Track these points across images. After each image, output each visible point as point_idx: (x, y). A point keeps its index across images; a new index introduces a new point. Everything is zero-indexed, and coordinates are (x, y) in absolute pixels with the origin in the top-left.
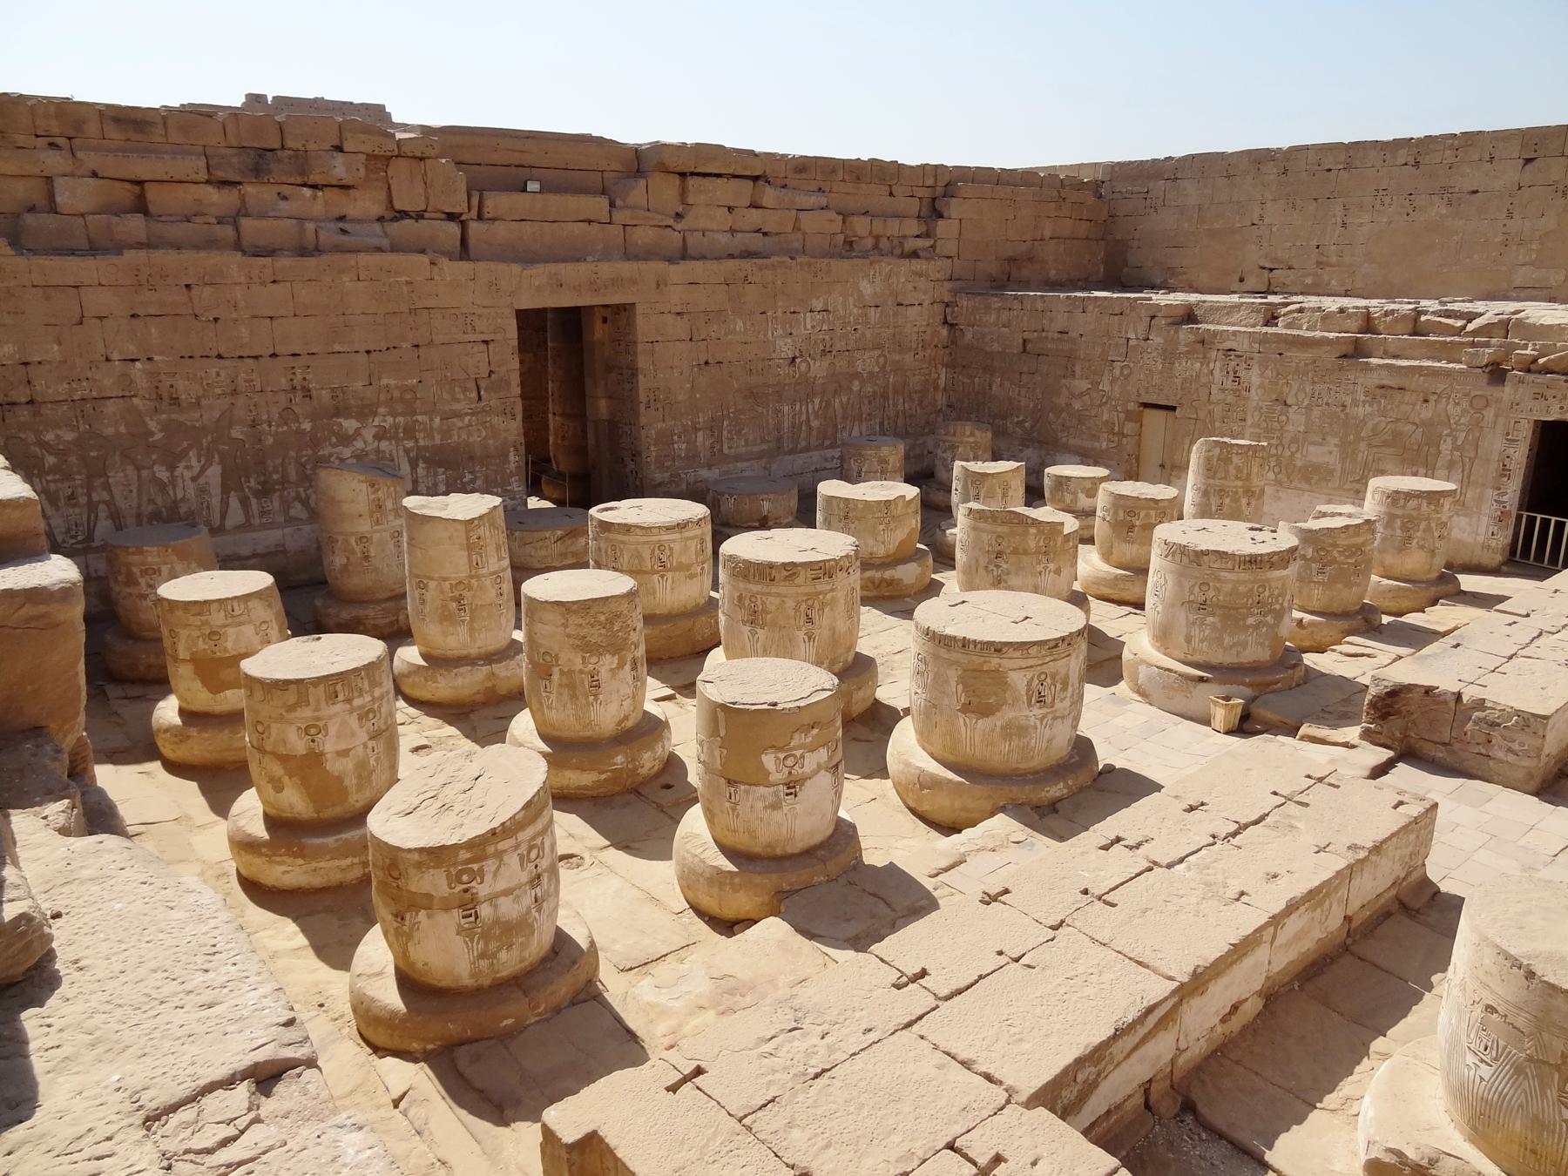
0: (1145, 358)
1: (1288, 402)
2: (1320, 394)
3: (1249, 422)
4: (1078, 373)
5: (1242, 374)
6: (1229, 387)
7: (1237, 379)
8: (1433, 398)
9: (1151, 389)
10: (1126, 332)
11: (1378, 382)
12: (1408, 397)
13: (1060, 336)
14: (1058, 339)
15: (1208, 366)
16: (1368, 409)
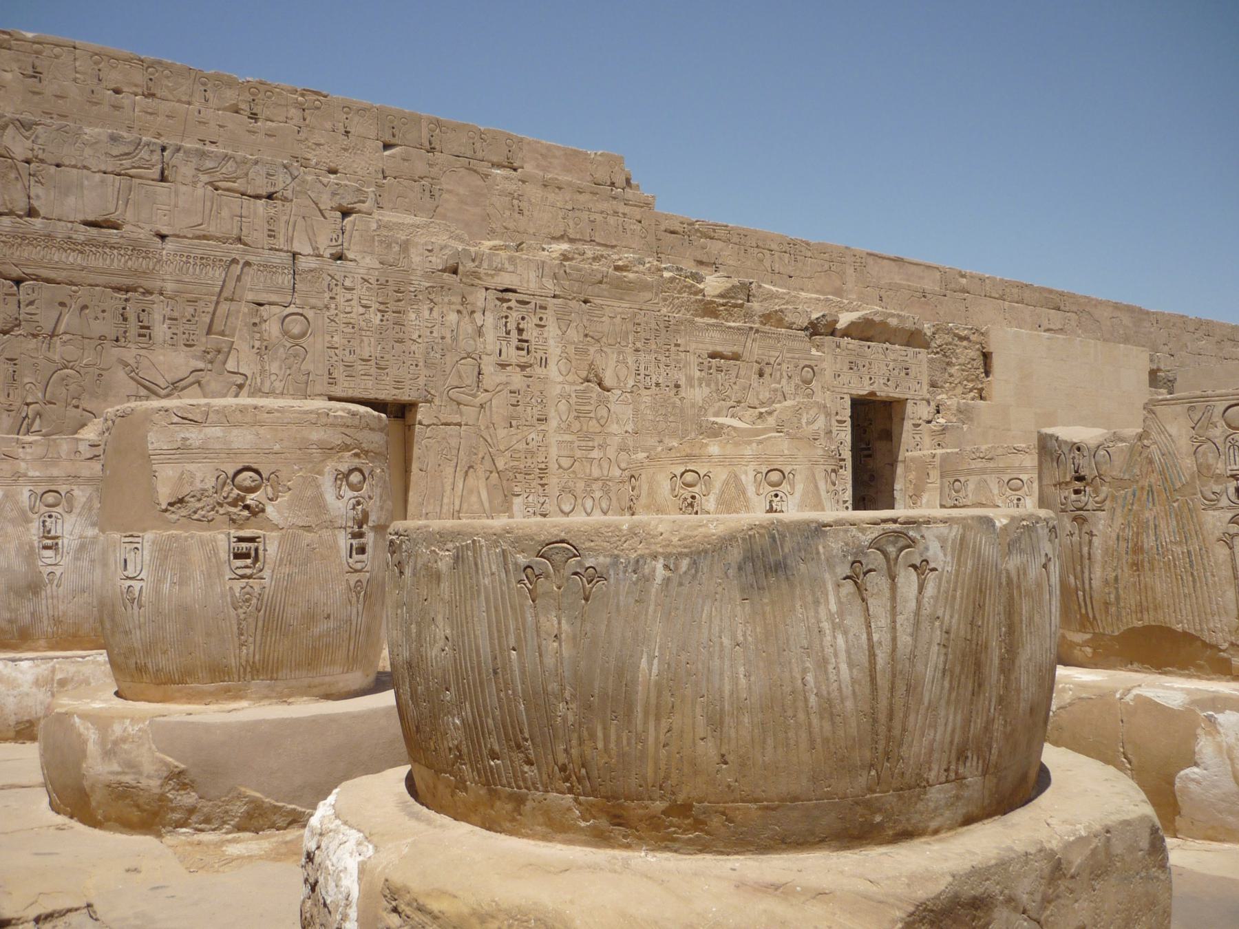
0: (341, 299)
1: (608, 382)
2: (646, 368)
3: (553, 423)
4: (161, 330)
5: (531, 333)
6: (514, 361)
7: (523, 345)
8: (768, 370)
9: (360, 367)
10: (290, 240)
11: (711, 349)
12: (747, 372)
13: (93, 231)
14: (89, 242)
15: (473, 321)
16: (706, 390)
